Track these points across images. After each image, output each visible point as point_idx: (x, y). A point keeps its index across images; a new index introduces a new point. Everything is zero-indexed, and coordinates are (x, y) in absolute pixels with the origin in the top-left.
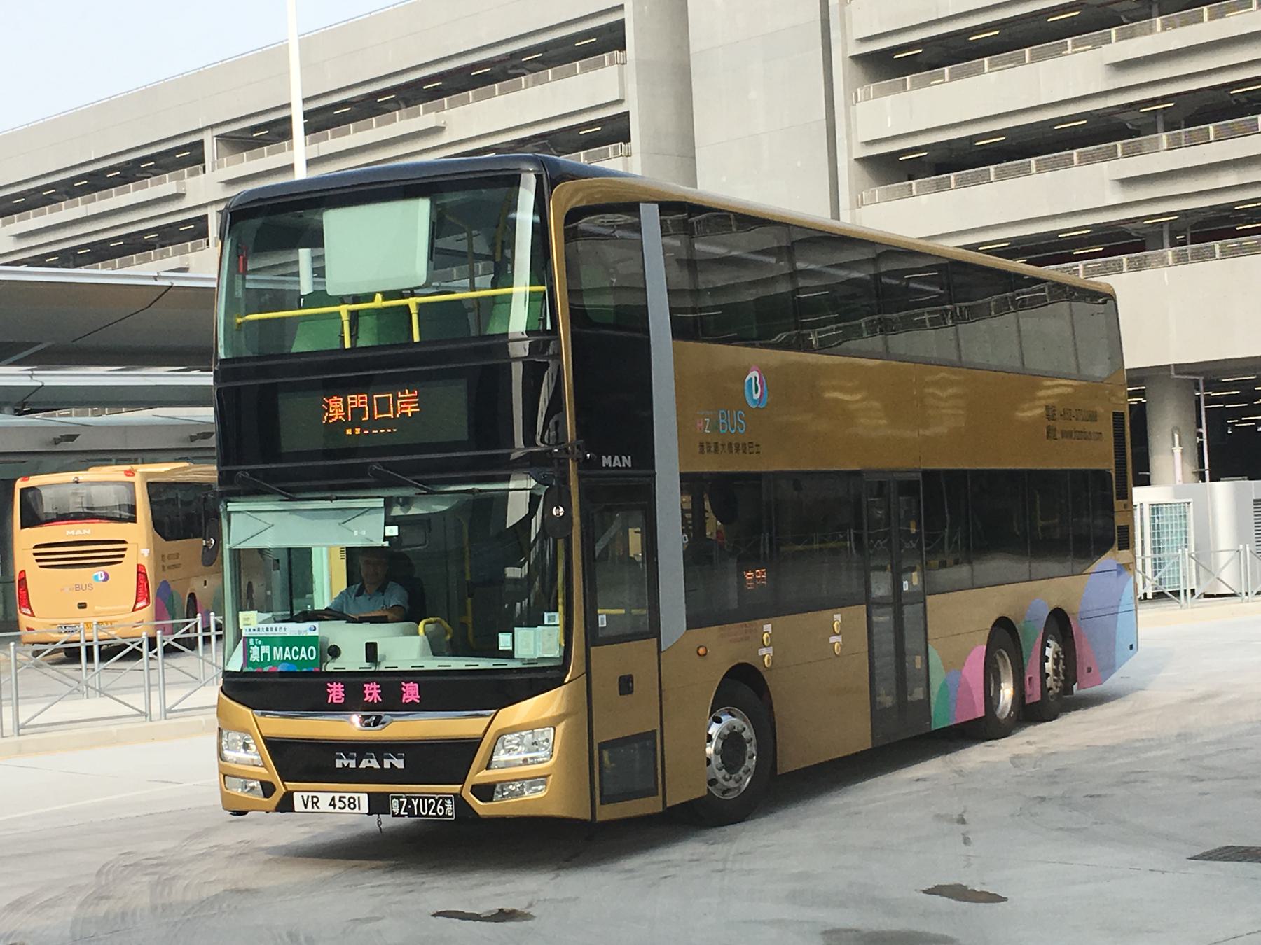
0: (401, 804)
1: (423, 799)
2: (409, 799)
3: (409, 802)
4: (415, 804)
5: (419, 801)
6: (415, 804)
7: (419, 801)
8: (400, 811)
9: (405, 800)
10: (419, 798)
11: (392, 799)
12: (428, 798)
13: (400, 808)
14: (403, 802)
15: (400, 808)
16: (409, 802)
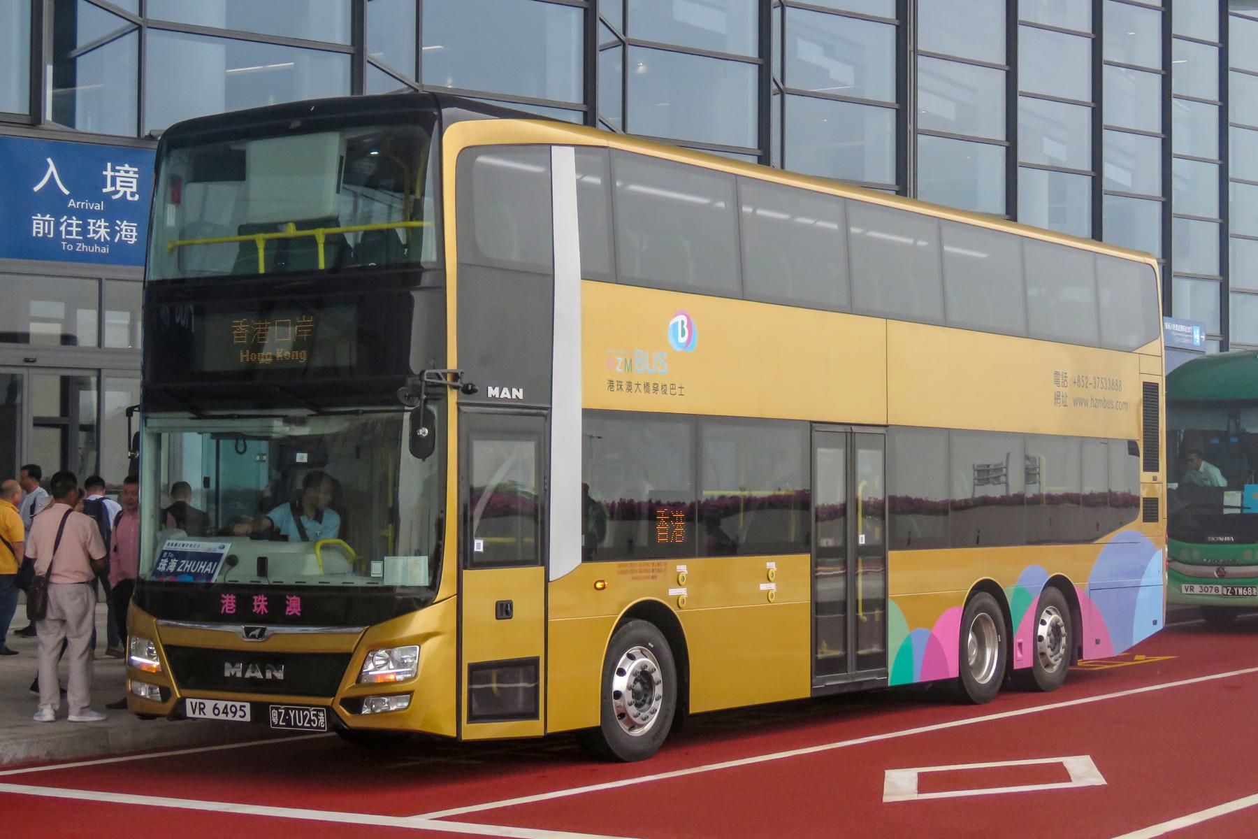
0: (280, 714)
1: (299, 710)
2: (287, 710)
3: (287, 714)
4: (292, 715)
5: (295, 712)
6: (292, 715)
7: (295, 712)
8: (279, 722)
9: (283, 711)
10: (294, 709)
11: (272, 710)
12: (304, 710)
13: (279, 718)
14: (282, 712)
16: (287, 714)
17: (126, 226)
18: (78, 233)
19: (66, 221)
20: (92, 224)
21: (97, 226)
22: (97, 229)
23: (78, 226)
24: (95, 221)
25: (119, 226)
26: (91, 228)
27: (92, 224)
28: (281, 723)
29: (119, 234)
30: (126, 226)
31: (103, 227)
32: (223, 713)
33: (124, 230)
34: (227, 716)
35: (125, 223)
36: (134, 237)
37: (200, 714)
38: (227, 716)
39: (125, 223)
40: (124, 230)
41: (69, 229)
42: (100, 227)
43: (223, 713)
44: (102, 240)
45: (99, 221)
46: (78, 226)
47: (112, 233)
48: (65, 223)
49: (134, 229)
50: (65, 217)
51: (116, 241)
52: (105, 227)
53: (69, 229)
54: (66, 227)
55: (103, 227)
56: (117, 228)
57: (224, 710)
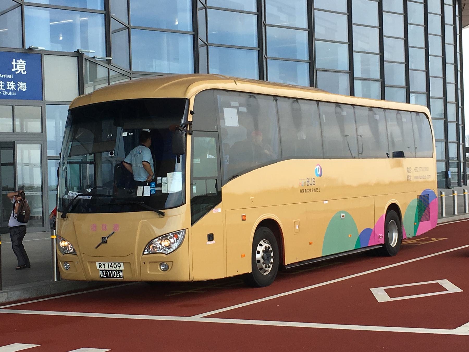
0: (103, 273)
3: (106, 272)
4: (109, 273)
5: (110, 272)
6: (109, 273)
7: (110, 272)
8: (103, 276)
9: (105, 271)
13: (103, 274)
14: (104, 272)
15: (103, 274)
16: (106, 272)
17: (22, 84)
18: (3, 87)
20: (8, 84)
21: (10, 84)
22: (11, 86)
23: (3, 84)
24: (9, 82)
25: (19, 84)
26: (8, 85)
27: (8, 84)
28: (104, 276)
29: (19, 88)
30: (22, 84)
31: (13, 85)
32: (110, 267)
33: (21, 86)
34: (112, 268)
35: (21, 83)
36: (25, 88)
37: (99, 268)
38: (112, 268)
39: (21, 83)
40: (21, 86)
42: (12, 85)
43: (110, 267)
44: (13, 90)
45: (11, 82)
46: (3, 84)
47: (17, 87)
49: (25, 85)
51: (18, 90)
52: (14, 85)
55: (13, 85)
56: (18, 85)
57: (111, 266)
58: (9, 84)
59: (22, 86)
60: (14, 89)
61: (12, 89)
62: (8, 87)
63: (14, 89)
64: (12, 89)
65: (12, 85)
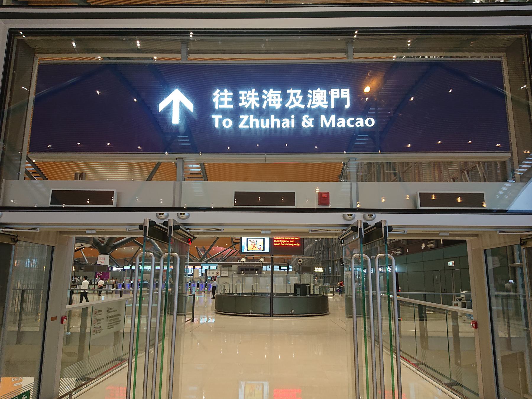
18: (229, 103)
19: (219, 93)
20: (243, 95)
21: (248, 96)
22: (248, 99)
23: (229, 96)
24: (246, 92)
25: (266, 95)
26: (242, 98)
27: (243, 95)
29: (265, 102)
31: (253, 96)
36: (279, 102)
39: (271, 91)
40: (270, 98)
41: (222, 99)
42: (250, 96)
44: (253, 108)
45: (249, 92)
46: (229, 96)
47: (261, 101)
48: (218, 95)
49: (279, 96)
50: (218, 91)
51: (264, 107)
52: (255, 96)
53: (222, 99)
54: (219, 98)
55: (253, 96)
56: (263, 97)
58: (246, 95)
59: (272, 98)
60: (255, 106)
61: (250, 106)
62: (243, 101)
63: (255, 106)
64: (250, 106)
65: (250, 96)
